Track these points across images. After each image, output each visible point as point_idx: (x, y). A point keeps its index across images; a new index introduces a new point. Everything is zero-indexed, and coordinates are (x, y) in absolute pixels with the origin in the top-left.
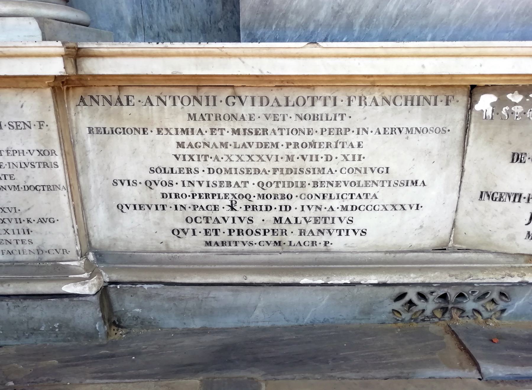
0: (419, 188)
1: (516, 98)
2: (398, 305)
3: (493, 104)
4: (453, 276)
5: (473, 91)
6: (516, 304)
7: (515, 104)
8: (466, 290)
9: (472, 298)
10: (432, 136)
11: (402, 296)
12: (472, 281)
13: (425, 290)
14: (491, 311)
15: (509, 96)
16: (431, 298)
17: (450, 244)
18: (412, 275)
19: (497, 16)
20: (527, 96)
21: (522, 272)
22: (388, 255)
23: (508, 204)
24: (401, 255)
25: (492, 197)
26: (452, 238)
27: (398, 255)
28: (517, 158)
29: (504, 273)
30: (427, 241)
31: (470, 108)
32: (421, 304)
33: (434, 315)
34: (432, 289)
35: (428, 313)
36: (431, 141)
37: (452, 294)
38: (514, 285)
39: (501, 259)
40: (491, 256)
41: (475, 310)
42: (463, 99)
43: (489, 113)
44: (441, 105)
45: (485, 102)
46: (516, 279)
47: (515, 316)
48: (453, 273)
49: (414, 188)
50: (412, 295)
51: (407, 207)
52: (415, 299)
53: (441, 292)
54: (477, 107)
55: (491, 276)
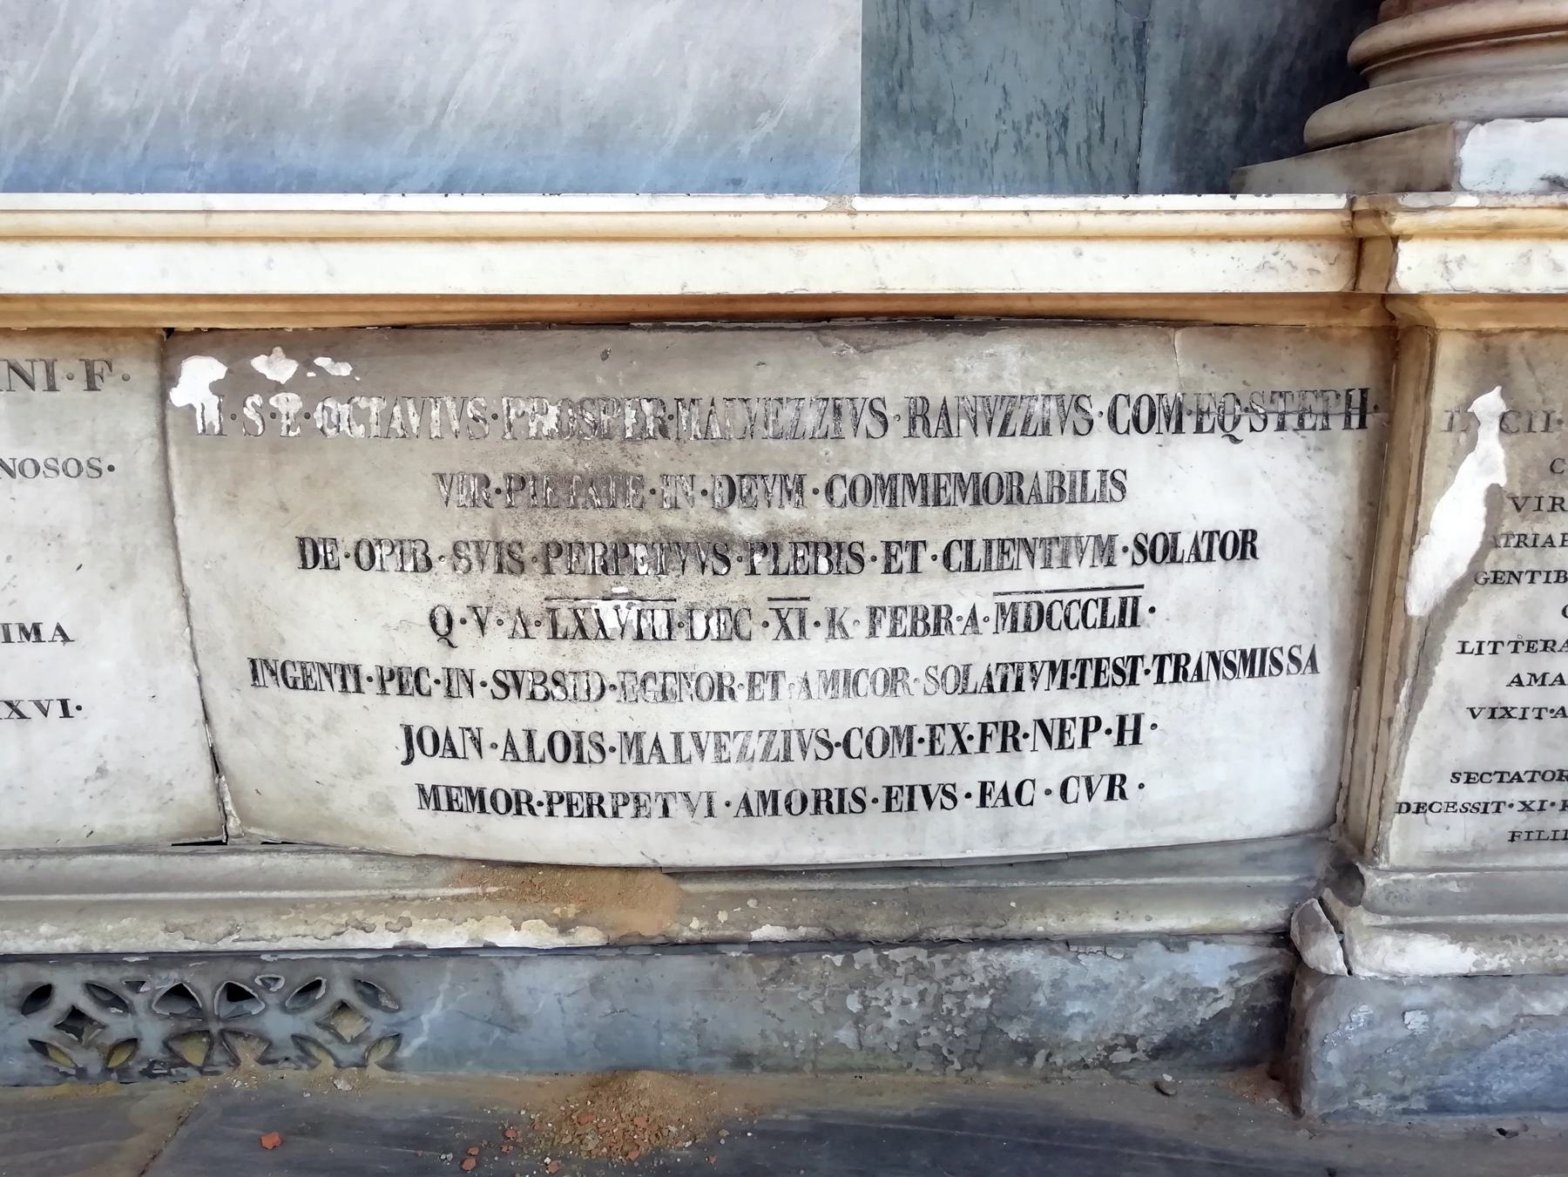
0: (50, 650)
1: (277, 367)
2: (41, 1025)
3: (216, 388)
4: (176, 928)
5: (170, 343)
6: (425, 1018)
7: (278, 387)
8: (242, 974)
9: (272, 1000)
10: (57, 485)
11: (40, 996)
12: (240, 946)
13: (109, 977)
14: (356, 1041)
15: (259, 363)
16: (138, 1000)
17: (233, 824)
18: (44, 929)
19: (138, 121)
20: (307, 364)
21: (405, 914)
22: (12, 862)
23: (329, 698)
24: (55, 861)
25: (280, 673)
26: (229, 807)
27: (44, 863)
28: (312, 554)
29: (344, 918)
30: (139, 817)
31: (163, 397)
32: (117, 1025)
33: (175, 1054)
34: (131, 974)
35: (151, 1045)
36: (58, 499)
37: (206, 989)
38: (387, 955)
39: (374, 873)
40: (345, 863)
41: (299, 1040)
42: (144, 372)
43: (213, 415)
44: (71, 391)
45: (198, 378)
46: (389, 941)
47: (434, 1056)
48: (180, 919)
49: (30, 647)
50: (69, 991)
51: (28, 709)
52: (86, 1005)
53: (168, 979)
54: (178, 397)
55: (301, 929)
